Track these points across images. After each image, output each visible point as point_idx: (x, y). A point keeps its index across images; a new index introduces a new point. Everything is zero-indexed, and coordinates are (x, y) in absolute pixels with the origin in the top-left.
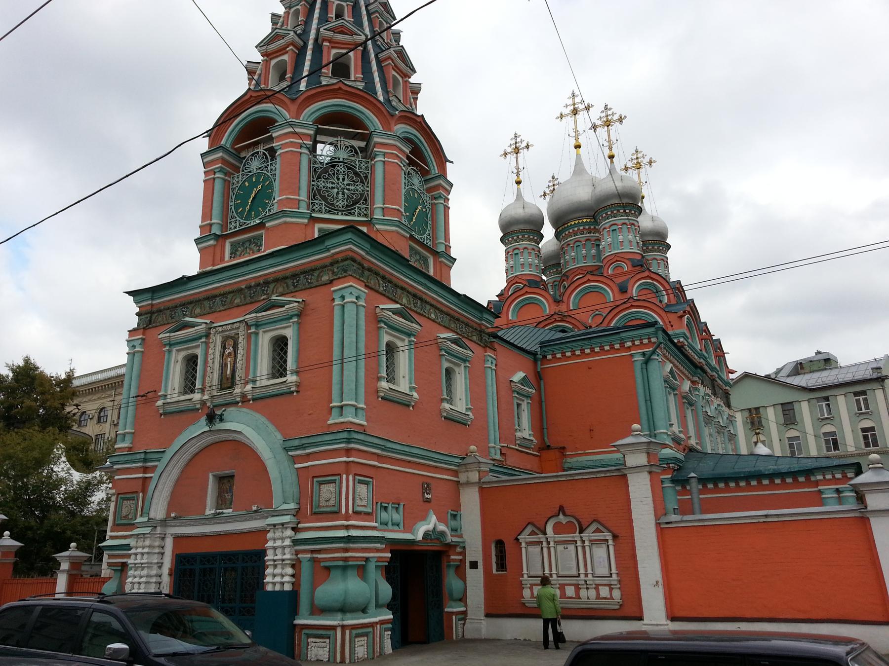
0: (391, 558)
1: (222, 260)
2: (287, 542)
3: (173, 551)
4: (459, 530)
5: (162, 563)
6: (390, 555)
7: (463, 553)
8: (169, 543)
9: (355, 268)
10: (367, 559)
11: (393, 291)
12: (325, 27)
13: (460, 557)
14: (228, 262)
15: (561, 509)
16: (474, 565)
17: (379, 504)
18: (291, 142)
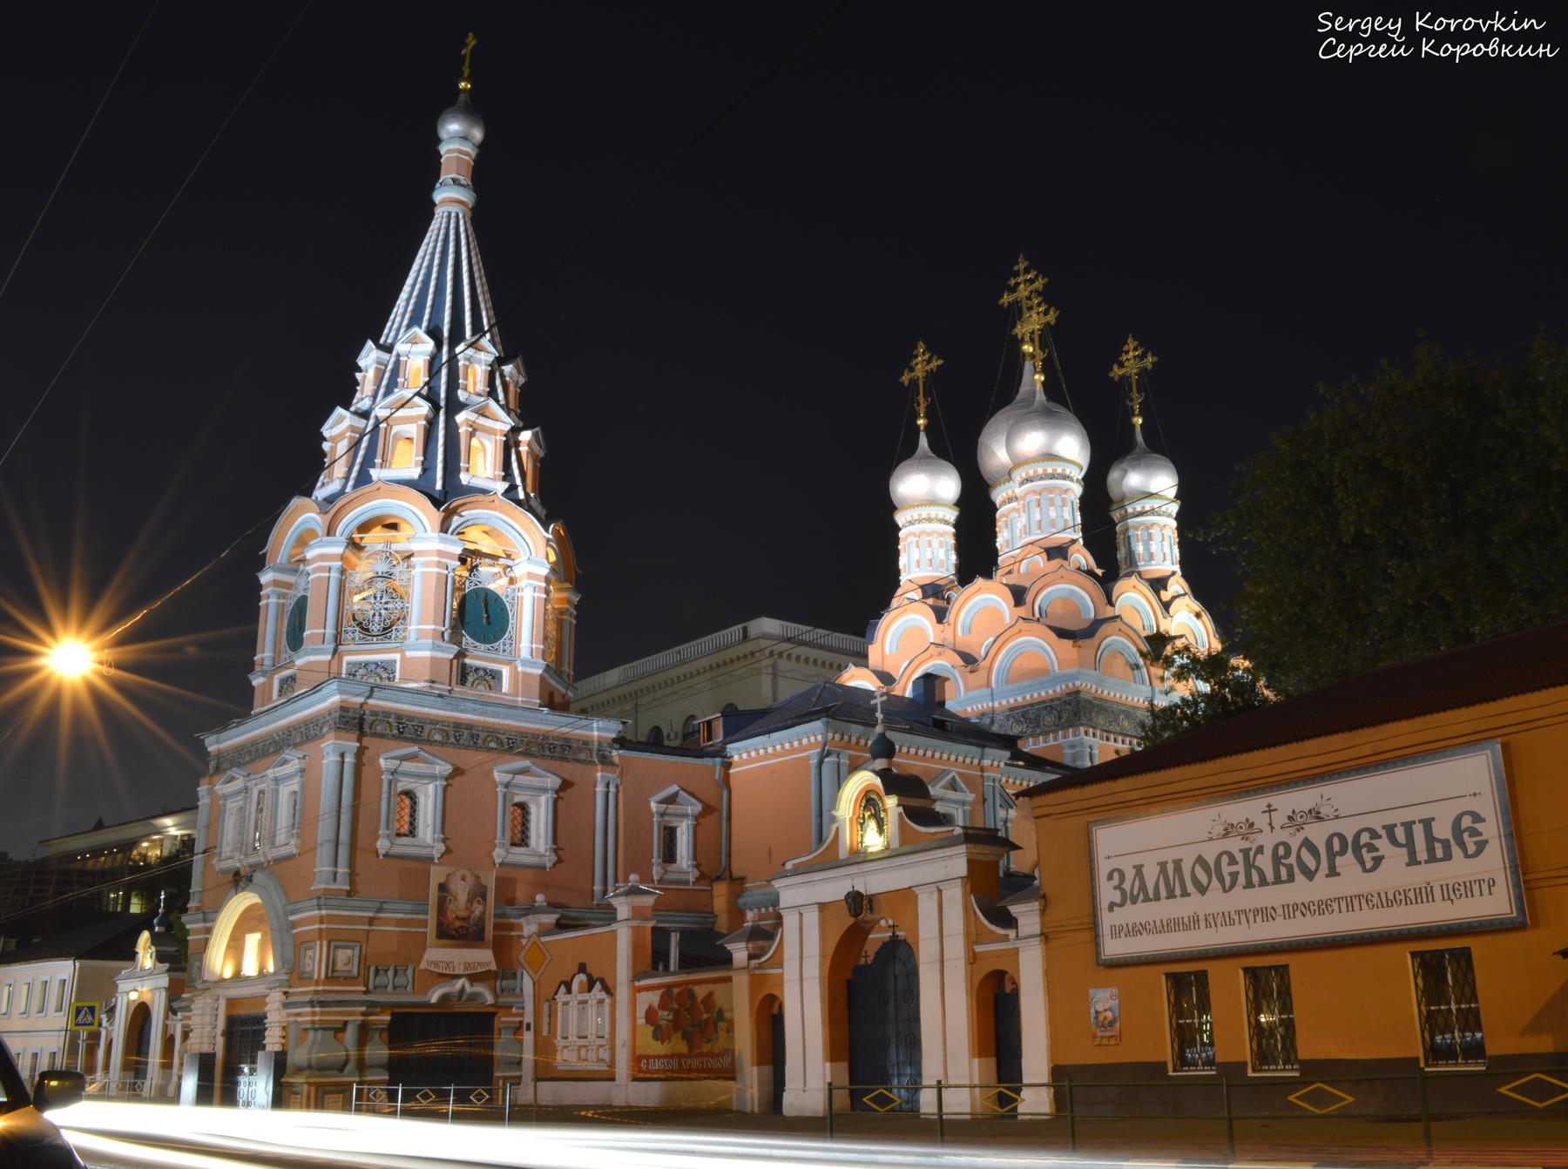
0: (391, 1021)
1: (270, 700)
2: (278, 1005)
3: (226, 1012)
4: (518, 991)
5: (216, 1025)
6: (389, 1018)
7: (522, 1015)
8: (222, 1004)
9: (347, 719)
10: (345, 1023)
11: (417, 730)
12: (380, 406)
13: (518, 1019)
14: (276, 701)
15: (582, 968)
16: (528, 1028)
17: (372, 969)
18: (320, 567)
